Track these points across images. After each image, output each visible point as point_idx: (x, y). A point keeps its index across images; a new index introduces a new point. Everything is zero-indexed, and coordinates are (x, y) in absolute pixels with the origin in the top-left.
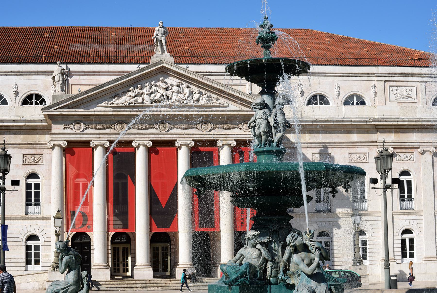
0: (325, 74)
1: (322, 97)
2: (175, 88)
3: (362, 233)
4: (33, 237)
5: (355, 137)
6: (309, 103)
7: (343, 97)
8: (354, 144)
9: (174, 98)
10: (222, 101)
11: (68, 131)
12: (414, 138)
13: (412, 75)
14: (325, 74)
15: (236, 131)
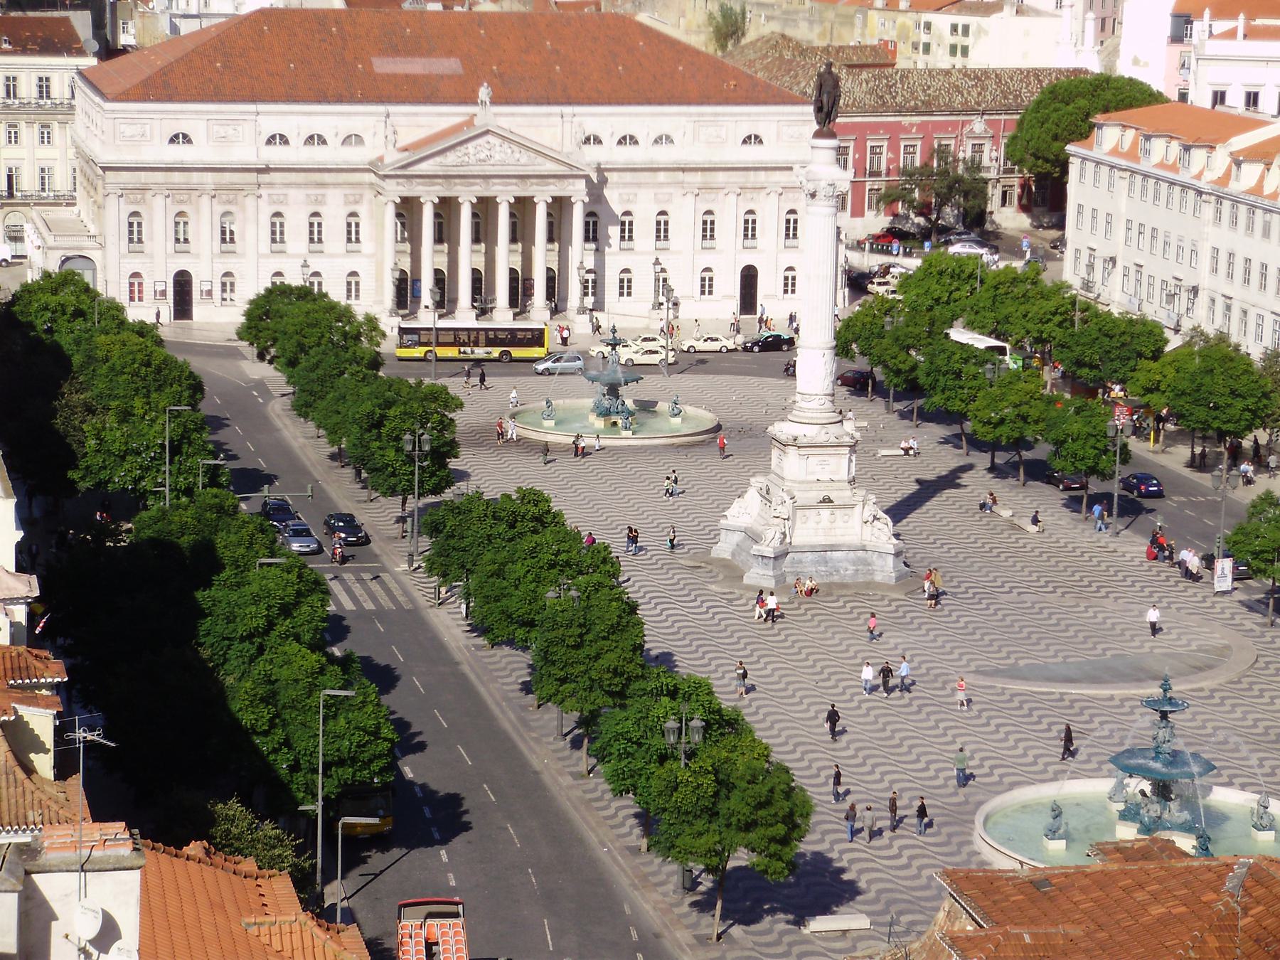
0: (637, 115)
1: (632, 137)
2: (498, 148)
3: (663, 270)
4: (354, 274)
5: (662, 176)
6: (620, 142)
7: (653, 137)
8: (661, 184)
9: (497, 157)
10: (540, 159)
11: (401, 188)
12: (721, 177)
13: (724, 115)
14: (637, 115)
15: (552, 187)
